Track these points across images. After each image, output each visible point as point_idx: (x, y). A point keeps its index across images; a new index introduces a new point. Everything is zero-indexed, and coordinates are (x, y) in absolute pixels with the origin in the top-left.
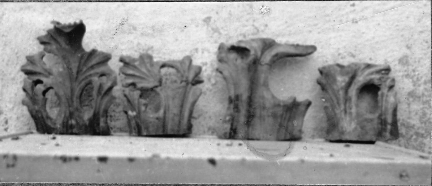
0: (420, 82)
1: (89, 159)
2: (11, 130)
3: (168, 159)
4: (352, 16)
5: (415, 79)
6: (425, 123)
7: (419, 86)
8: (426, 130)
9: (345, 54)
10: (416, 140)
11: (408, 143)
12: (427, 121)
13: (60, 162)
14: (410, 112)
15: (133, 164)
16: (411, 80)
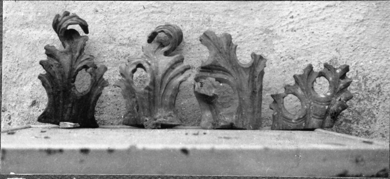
3: (144, 149)
4: (291, 26)
6: (353, 112)
9: (286, 57)
10: (345, 126)
12: (354, 110)
15: (113, 154)
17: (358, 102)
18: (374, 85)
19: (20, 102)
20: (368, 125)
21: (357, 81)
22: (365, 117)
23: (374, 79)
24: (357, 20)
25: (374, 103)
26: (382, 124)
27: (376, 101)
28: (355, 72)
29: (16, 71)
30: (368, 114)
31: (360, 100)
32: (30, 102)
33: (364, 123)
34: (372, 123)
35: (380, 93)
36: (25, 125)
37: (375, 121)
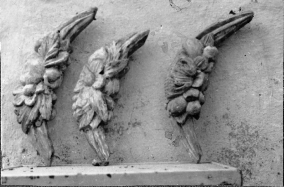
0: (235, 128)
2: (11, 165)
5: (232, 126)
7: (235, 129)
8: (240, 153)
10: (234, 159)
11: (230, 161)
12: (240, 148)
14: (230, 144)
16: (230, 127)
17: (243, 143)
18: (253, 131)
19: (15, 150)
20: (250, 158)
21: (242, 129)
22: (248, 153)
23: (254, 128)
24: (241, 88)
25: (253, 144)
26: (260, 157)
27: (255, 142)
28: (241, 123)
29: (11, 130)
30: (250, 151)
32: (20, 150)
33: (248, 157)
34: (253, 157)
35: (258, 137)
36: (18, 165)
37: (255, 155)
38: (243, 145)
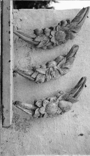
1: (9, 29)
13: (9, 21)
18: (27, 130)
31: (22, 125)
32: (21, 18)
36: (14, 17)
38: (21, 125)
